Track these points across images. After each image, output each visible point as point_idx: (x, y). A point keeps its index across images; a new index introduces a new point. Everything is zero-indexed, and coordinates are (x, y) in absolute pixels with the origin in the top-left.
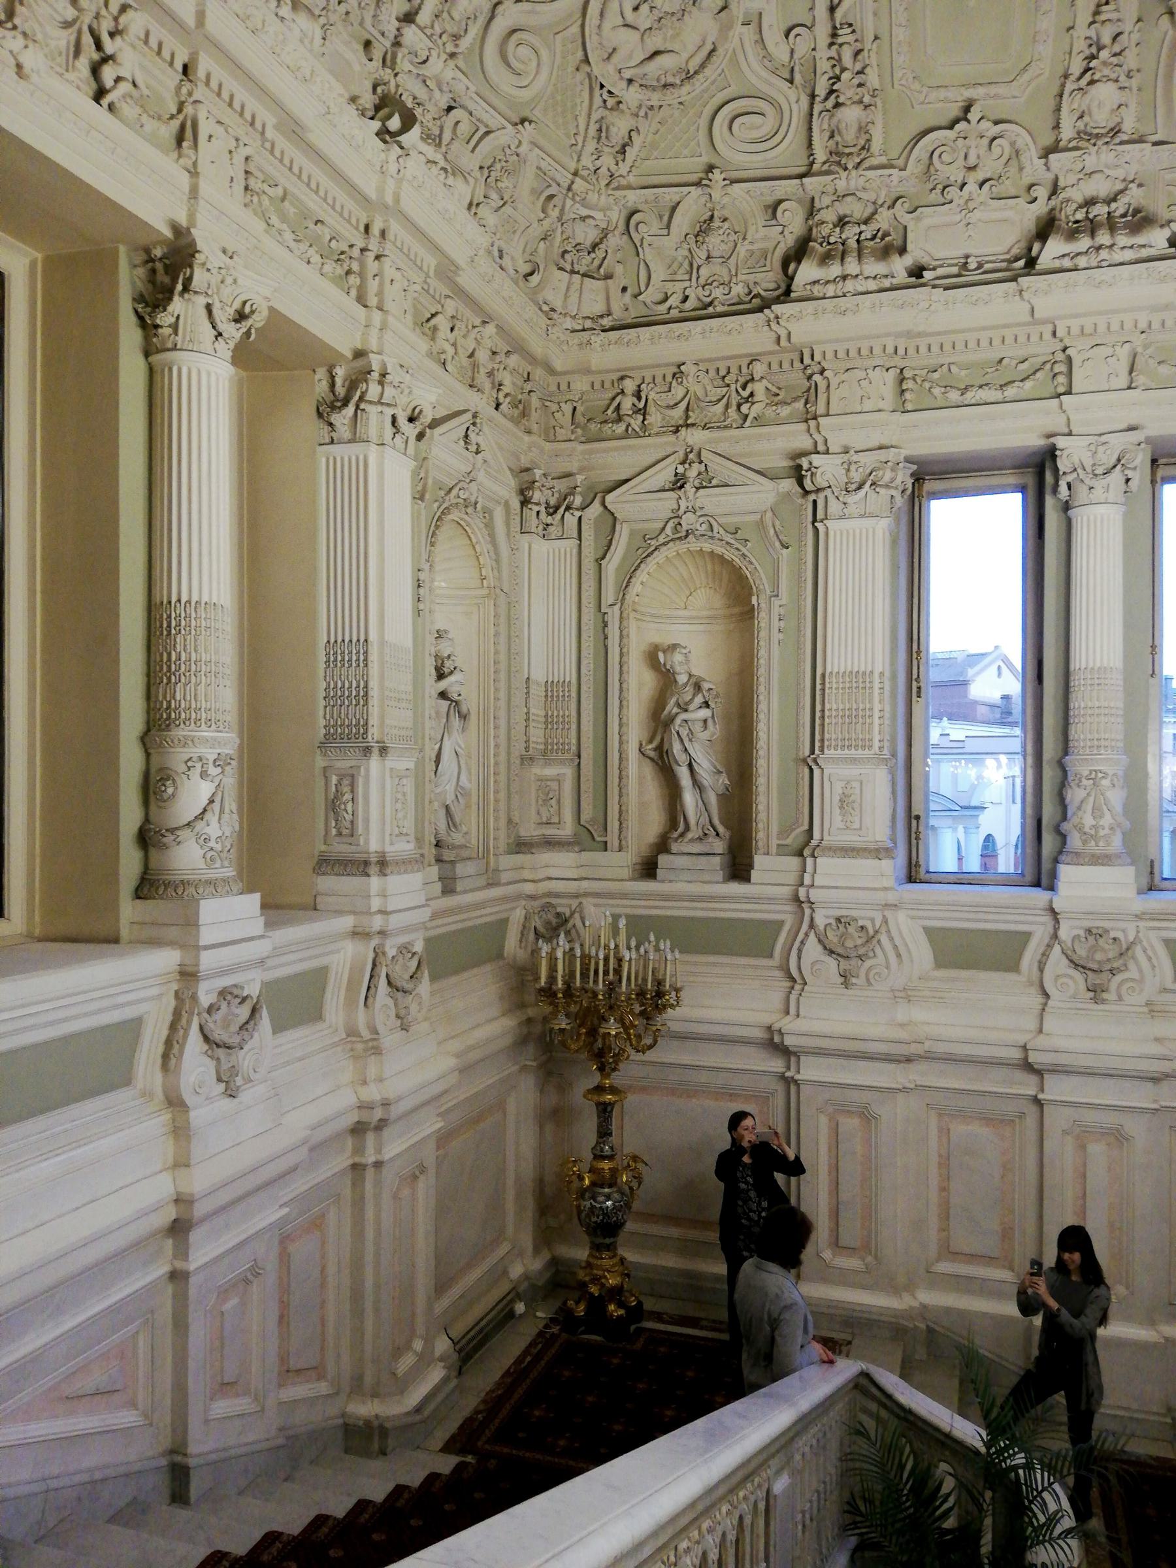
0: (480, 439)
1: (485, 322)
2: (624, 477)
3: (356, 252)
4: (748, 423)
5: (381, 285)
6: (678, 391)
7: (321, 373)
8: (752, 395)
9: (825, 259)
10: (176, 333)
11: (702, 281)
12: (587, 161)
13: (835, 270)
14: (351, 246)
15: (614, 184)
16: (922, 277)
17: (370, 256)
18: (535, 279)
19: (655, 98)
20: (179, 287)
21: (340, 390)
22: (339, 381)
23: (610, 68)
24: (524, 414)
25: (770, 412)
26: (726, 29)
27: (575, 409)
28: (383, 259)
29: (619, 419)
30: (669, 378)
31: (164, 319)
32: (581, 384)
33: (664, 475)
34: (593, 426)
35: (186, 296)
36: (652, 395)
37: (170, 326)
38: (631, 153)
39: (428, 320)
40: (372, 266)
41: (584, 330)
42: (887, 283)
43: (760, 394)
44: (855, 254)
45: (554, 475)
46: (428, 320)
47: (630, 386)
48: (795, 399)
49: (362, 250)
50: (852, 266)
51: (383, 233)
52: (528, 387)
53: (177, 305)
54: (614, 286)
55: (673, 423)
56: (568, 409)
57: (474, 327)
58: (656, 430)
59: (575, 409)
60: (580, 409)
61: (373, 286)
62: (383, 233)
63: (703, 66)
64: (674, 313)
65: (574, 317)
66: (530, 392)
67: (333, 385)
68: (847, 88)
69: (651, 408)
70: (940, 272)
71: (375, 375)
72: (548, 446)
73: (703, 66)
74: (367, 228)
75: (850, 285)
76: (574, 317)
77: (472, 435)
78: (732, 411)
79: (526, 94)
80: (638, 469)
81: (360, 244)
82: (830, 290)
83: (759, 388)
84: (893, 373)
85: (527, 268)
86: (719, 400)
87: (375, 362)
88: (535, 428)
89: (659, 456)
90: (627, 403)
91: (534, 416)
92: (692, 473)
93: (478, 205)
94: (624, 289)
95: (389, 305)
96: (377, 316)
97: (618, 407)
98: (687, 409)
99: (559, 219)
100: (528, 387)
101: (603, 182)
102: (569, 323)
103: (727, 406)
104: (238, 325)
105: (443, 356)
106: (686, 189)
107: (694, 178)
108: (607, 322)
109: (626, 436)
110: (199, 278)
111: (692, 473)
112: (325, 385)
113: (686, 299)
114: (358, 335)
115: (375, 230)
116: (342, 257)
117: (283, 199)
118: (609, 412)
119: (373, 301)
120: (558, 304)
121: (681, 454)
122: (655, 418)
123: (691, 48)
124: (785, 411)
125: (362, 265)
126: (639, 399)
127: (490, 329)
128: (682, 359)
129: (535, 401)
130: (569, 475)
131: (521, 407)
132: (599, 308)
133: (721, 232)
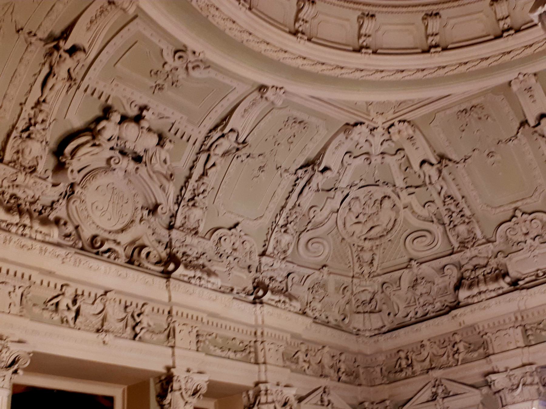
0: (330, 398)
1: (324, 347)
2: (410, 397)
3: (252, 344)
4: (459, 363)
5: (265, 352)
6: (425, 354)
7: (244, 395)
8: (458, 349)
9: (470, 287)
10: (170, 406)
11: (422, 304)
12: (357, 270)
13: (475, 291)
14: (250, 342)
15: (371, 276)
16: (518, 284)
17: (258, 343)
18: (347, 321)
19: (378, 242)
20: (170, 390)
21: (252, 400)
22: (251, 396)
23: (355, 237)
24: (357, 376)
25: (469, 356)
26: (398, 212)
27: (381, 369)
28: (264, 343)
29: (401, 371)
30: (419, 347)
31: (166, 402)
32: (381, 358)
33: (427, 394)
34: (392, 376)
35: (172, 392)
36: (413, 357)
37: (168, 404)
38: (375, 263)
39: (294, 355)
40: (260, 347)
41: (375, 335)
42: (500, 291)
43: (462, 349)
44: (483, 281)
45: (378, 401)
46: (294, 355)
47: (402, 354)
48: (479, 348)
49: (255, 342)
50: (483, 288)
51: (262, 333)
52: (356, 364)
53: (169, 397)
54: (384, 314)
55: (426, 368)
56: (378, 369)
57: (319, 350)
58: (418, 373)
59: (381, 369)
60: (384, 368)
61: (261, 355)
62: (262, 333)
63: (394, 226)
64: (413, 320)
65: (370, 330)
66: (358, 366)
67: (249, 398)
68: (457, 219)
69: (415, 363)
70: (527, 280)
71: (263, 392)
72: (372, 389)
73: (394, 226)
74: (255, 333)
75: (483, 296)
76: (370, 330)
77: (326, 398)
78: (450, 358)
79: (322, 258)
80: (415, 392)
81: (254, 340)
82: (476, 300)
83: (461, 346)
84: (520, 329)
85: (343, 317)
86: (444, 354)
87: (262, 387)
88: (364, 382)
89: (424, 384)
90: (404, 363)
91: (362, 377)
92: (440, 391)
93: (310, 303)
94: (389, 314)
95: (268, 360)
96: (263, 367)
97: (400, 365)
98: (430, 361)
99: (352, 293)
100: (356, 364)
101: (366, 277)
102: (368, 334)
103: (448, 356)
104: (194, 396)
105: (303, 369)
106: (401, 271)
107: (405, 265)
108: (384, 329)
109: (406, 378)
110: (176, 385)
111: (440, 391)
112: (246, 398)
113: (416, 313)
114: (257, 376)
115: (259, 333)
116: (246, 347)
117: (216, 337)
118: (397, 367)
119: (261, 360)
120: (360, 327)
121: (433, 382)
122: (417, 367)
123: (386, 222)
124: (475, 355)
125: (256, 349)
126: (408, 359)
127: (326, 349)
128: (422, 340)
129: (361, 370)
130: (384, 401)
131: (354, 374)
132: (380, 324)
133: (422, 284)
